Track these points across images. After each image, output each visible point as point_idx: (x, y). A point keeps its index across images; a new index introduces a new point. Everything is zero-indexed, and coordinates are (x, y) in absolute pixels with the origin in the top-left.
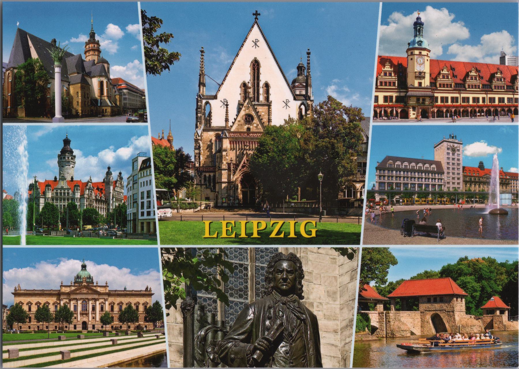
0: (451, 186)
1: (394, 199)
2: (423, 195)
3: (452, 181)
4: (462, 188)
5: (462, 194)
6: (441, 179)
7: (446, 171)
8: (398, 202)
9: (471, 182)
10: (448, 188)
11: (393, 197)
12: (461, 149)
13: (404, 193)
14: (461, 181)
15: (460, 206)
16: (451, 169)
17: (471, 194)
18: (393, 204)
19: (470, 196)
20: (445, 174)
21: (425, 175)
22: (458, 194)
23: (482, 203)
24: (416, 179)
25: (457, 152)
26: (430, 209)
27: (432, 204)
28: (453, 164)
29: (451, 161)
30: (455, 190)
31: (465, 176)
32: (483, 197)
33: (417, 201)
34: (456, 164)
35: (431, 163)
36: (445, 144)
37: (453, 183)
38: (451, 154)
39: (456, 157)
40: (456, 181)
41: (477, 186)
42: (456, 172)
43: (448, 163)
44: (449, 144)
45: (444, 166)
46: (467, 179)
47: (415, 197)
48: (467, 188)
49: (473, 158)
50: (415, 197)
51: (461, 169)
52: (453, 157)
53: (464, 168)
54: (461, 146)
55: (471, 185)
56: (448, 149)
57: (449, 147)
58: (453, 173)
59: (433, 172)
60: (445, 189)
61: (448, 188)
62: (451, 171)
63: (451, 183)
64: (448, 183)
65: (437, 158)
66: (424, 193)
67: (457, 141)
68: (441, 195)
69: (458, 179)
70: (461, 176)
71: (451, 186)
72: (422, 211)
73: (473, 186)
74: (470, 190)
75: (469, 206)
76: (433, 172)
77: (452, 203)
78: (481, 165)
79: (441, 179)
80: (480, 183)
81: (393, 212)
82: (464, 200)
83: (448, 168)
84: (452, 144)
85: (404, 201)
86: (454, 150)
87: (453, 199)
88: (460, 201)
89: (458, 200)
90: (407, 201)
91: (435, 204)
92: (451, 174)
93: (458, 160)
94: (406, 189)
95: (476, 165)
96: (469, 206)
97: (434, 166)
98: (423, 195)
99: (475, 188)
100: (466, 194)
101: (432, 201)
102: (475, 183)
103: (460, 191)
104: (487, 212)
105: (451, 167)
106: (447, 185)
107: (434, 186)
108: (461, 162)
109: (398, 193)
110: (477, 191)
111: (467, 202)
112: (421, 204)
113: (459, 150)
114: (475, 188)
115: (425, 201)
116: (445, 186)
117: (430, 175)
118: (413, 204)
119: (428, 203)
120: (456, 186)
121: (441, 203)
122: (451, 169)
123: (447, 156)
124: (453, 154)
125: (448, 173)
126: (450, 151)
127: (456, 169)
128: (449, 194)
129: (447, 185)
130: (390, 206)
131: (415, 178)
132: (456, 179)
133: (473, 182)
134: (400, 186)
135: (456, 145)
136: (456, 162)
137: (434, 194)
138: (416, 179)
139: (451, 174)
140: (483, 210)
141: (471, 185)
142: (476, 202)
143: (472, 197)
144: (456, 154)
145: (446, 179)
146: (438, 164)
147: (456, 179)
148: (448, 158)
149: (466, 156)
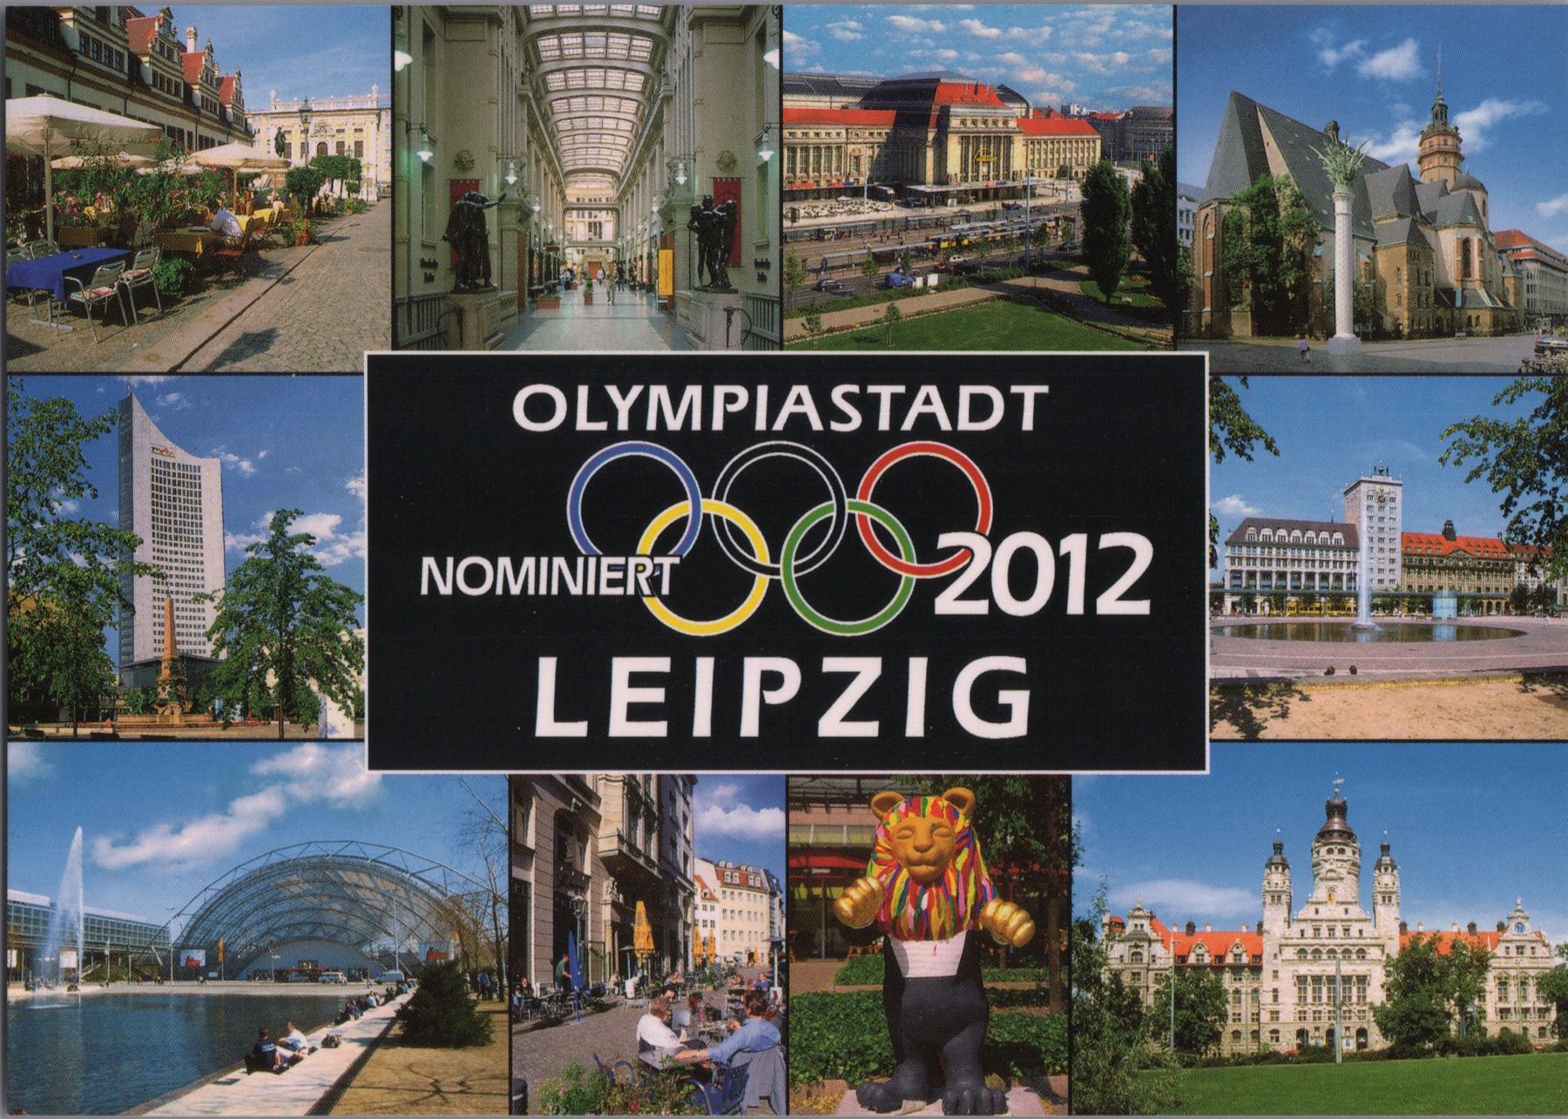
25: (1388, 505)
31: (1405, 554)
35: (1332, 528)
39: (1386, 513)
51: (1398, 540)
56: (1370, 497)
67: (1390, 480)
69: (1393, 561)
70: (1398, 556)
76: (1337, 548)
84: (1378, 487)
86: (1381, 500)
113: (1393, 500)
124: (1381, 508)
135: (1387, 489)
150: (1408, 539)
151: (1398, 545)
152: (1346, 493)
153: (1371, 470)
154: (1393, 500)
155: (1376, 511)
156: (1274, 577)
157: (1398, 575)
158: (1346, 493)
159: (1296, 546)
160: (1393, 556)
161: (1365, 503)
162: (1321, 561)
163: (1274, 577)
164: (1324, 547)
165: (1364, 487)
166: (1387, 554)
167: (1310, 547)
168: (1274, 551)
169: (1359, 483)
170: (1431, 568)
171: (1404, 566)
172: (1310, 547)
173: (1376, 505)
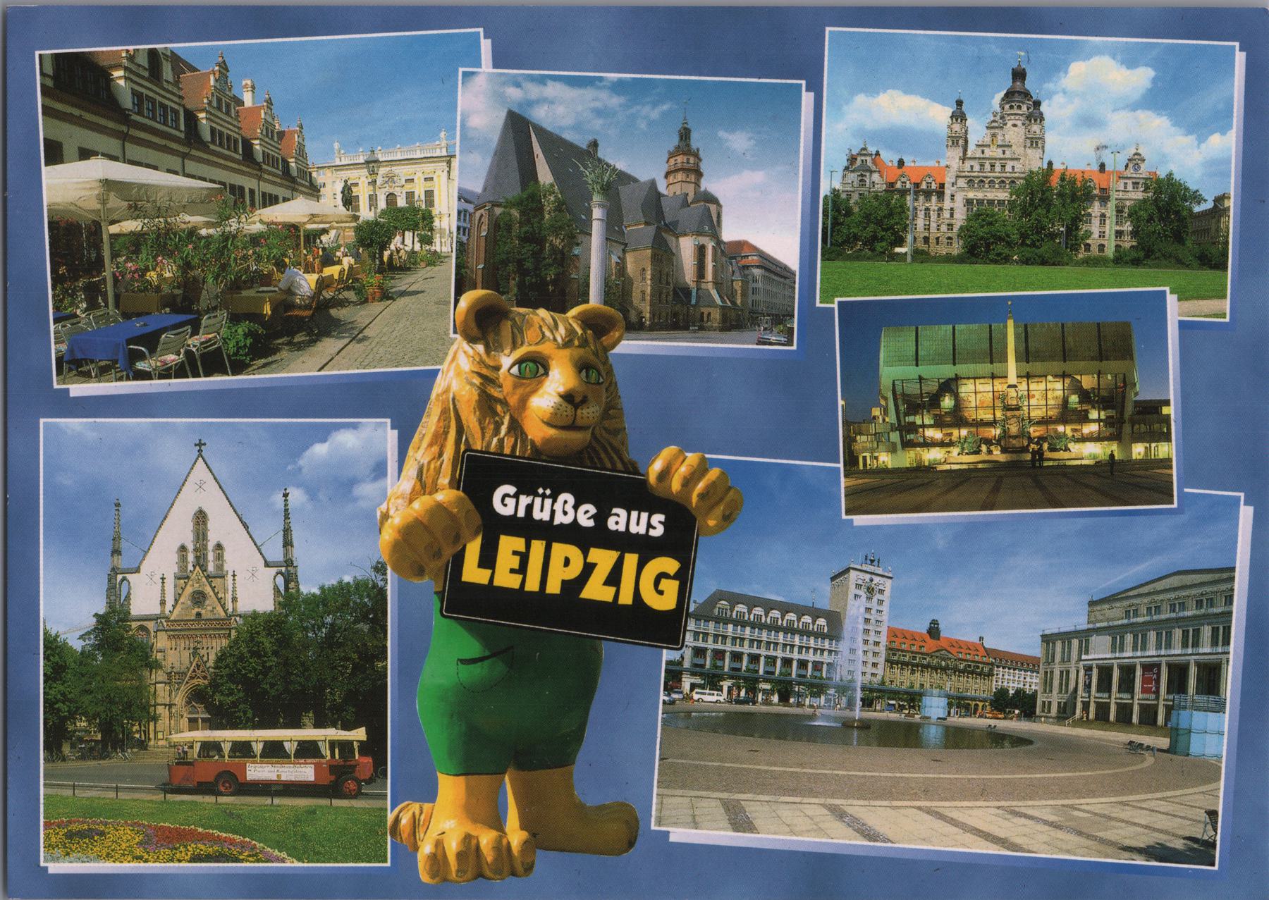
25: (878, 596)
31: (889, 649)
35: (816, 613)
40: (871, 659)
44: (861, 575)
56: (858, 586)
57: (860, 582)
67: (880, 571)
70: (882, 649)
76: (818, 635)
84: (867, 577)
86: (870, 590)
97: (822, 621)
113: (881, 592)
124: (869, 599)
126: (862, 592)
135: (877, 579)
144: (875, 600)
150: (893, 633)
151: (883, 639)
152: (833, 579)
153: (861, 559)
154: (881, 592)
156: (745, 659)
158: (833, 579)
160: (877, 649)
161: (852, 590)
163: (745, 659)
165: (853, 574)
166: (871, 647)
169: (847, 570)
170: (914, 667)
173: (864, 596)
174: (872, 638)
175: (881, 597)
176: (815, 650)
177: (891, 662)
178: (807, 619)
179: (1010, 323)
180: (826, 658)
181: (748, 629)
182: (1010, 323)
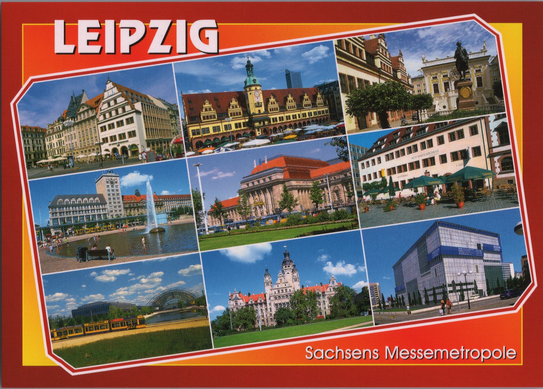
0: (114, 213)
1: (68, 232)
2: (91, 225)
3: (114, 209)
4: (123, 214)
5: (124, 219)
6: (105, 209)
7: (108, 201)
8: (71, 233)
9: (130, 208)
10: (112, 216)
11: (66, 230)
12: (118, 182)
13: (75, 225)
14: (122, 208)
15: (124, 229)
16: (112, 199)
17: (132, 218)
18: (67, 236)
19: (131, 220)
20: (108, 204)
21: (91, 207)
22: (121, 219)
23: (143, 224)
24: (84, 212)
25: (115, 184)
26: (99, 236)
27: (100, 232)
28: (114, 194)
29: (111, 192)
30: (118, 217)
31: (124, 204)
32: (143, 219)
33: (87, 231)
34: (116, 194)
36: (104, 178)
37: (116, 211)
38: (110, 187)
39: (115, 188)
40: (118, 209)
41: (136, 211)
42: (117, 201)
43: (109, 195)
45: (106, 197)
46: (127, 206)
47: (85, 228)
48: (128, 214)
49: (130, 188)
50: (85, 228)
51: (121, 198)
52: (113, 189)
53: (123, 196)
54: (118, 178)
55: (130, 210)
56: (107, 182)
58: (115, 203)
59: (97, 204)
60: (109, 217)
61: (112, 216)
62: (112, 200)
63: (114, 211)
64: (112, 211)
65: (99, 192)
66: (92, 223)
67: (114, 175)
68: (107, 223)
69: (119, 206)
71: (114, 213)
72: (92, 238)
73: (133, 211)
74: (130, 215)
75: (131, 229)
76: (97, 204)
77: (117, 229)
78: (137, 194)
79: (105, 209)
80: (138, 208)
81: (68, 243)
82: (127, 224)
83: (110, 199)
85: (76, 232)
86: (112, 183)
87: (117, 225)
88: (124, 225)
89: (122, 225)
90: (79, 232)
91: (102, 231)
92: (113, 203)
93: (117, 190)
94: (76, 222)
95: (133, 194)
96: (131, 229)
97: (97, 199)
98: (91, 225)
99: (135, 213)
100: (128, 219)
101: (100, 229)
102: (134, 208)
103: (122, 217)
104: (148, 232)
105: (112, 197)
106: (110, 214)
107: (99, 215)
108: (120, 192)
109: (71, 226)
110: (137, 215)
111: (130, 225)
112: (91, 233)
113: (116, 182)
114: (135, 213)
115: (94, 230)
116: (109, 214)
117: (95, 206)
118: (84, 234)
119: (96, 232)
120: (118, 213)
121: (108, 229)
122: (112, 199)
123: (107, 189)
124: (112, 186)
125: (110, 203)
127: (116, 199)
128: (113, 221)
129: (110, 214)
130: (65, 238)
131: (82, 211)
132: (117, 207)
133: (132, 208)
134: (71, 220)
135: (113, 178)
136: (115, 192)
137: (100, 222)
138: (84, 212)
139: (113, 203)
140: (144, 230)
141: (130, 210)
142: (137, 224)
143: (133, 221)
144: (114, 186)
145: (109, 209)
146: (101, 196)
147: (117, 207)
148: (109, 190)
149: (123, 188)
155: (110, 188)
157: (123, 212)
159: (80, 205)
160: (119, 205)
162: (92, 210)
164: (92, 204)
166: (117, 204)
167: (86, 205)
168: (71, 208)
171: (124, 208)
172: (86, 205)
173: (110, 185)
174: (117, 201)
175: (117, 184)
176: (97, 210)
177: (126, 208)
178: (91, 199)
179: (255, 161)
180: (102, 212)
181: (71, 208)
182: (255, 161)
